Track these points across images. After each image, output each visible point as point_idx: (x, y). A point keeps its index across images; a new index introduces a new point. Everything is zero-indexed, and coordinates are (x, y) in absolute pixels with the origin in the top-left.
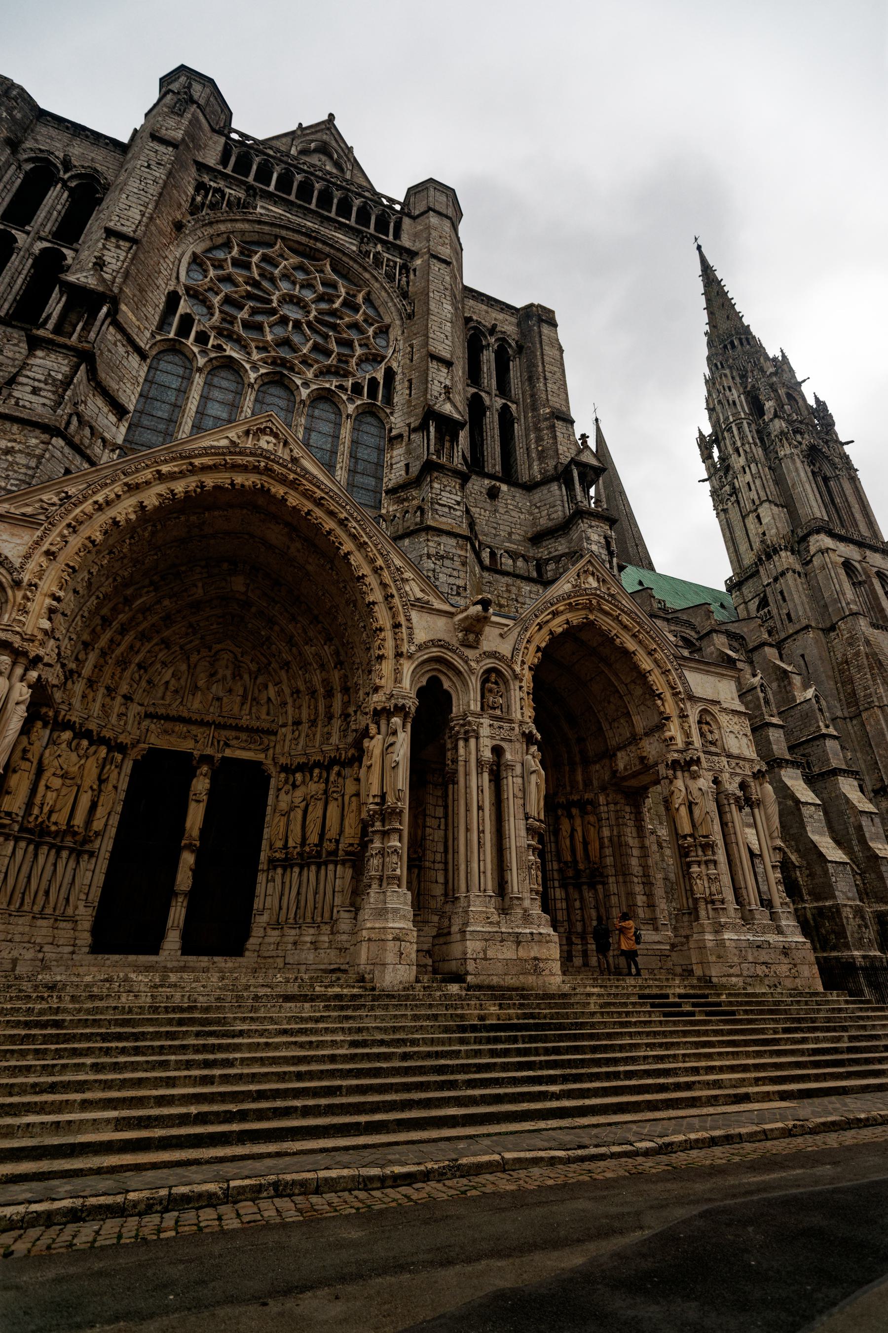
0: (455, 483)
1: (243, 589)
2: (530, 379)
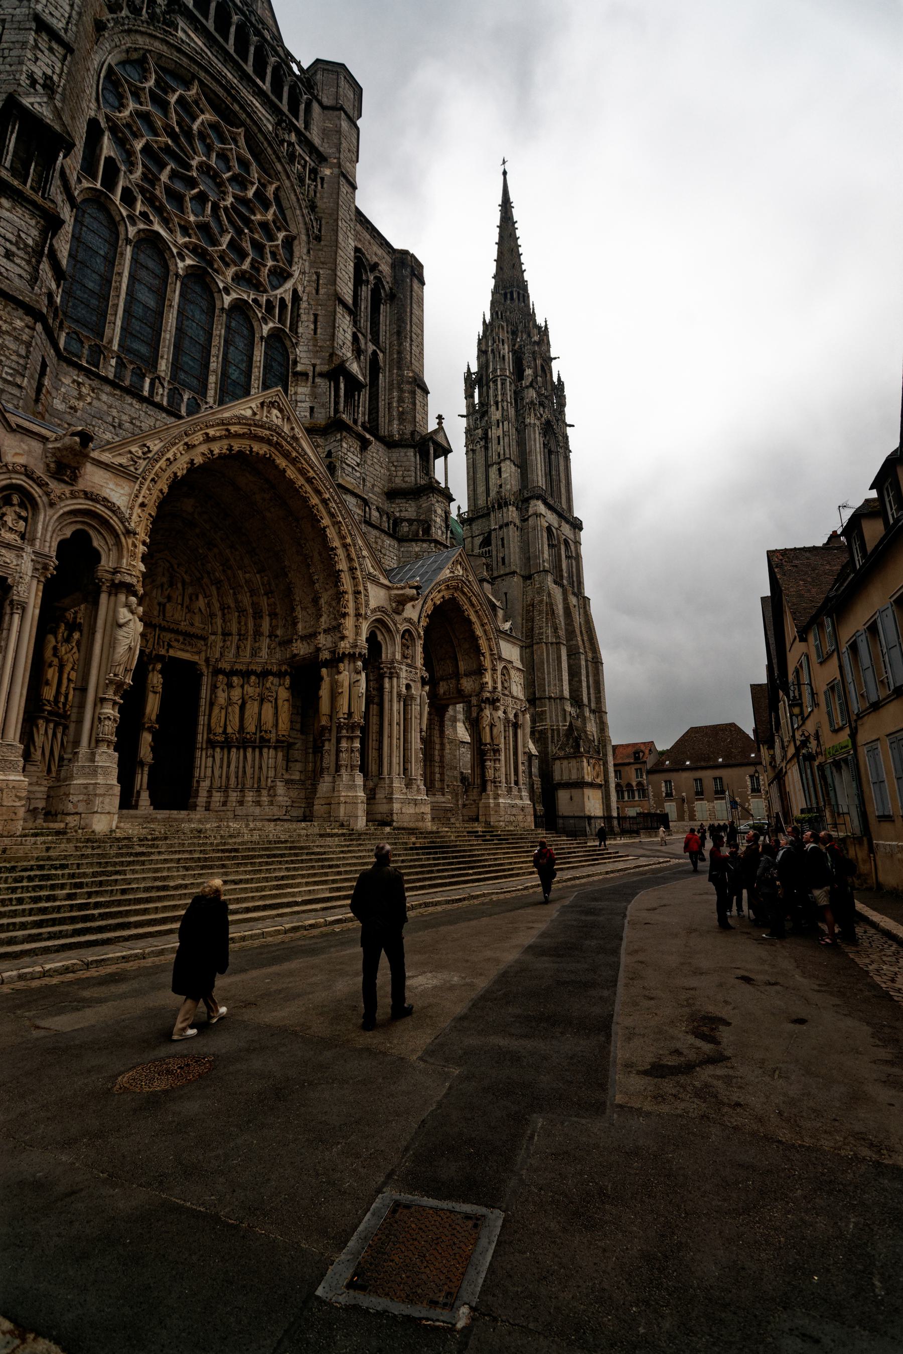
0: (356, 445)
2: (399, 333)
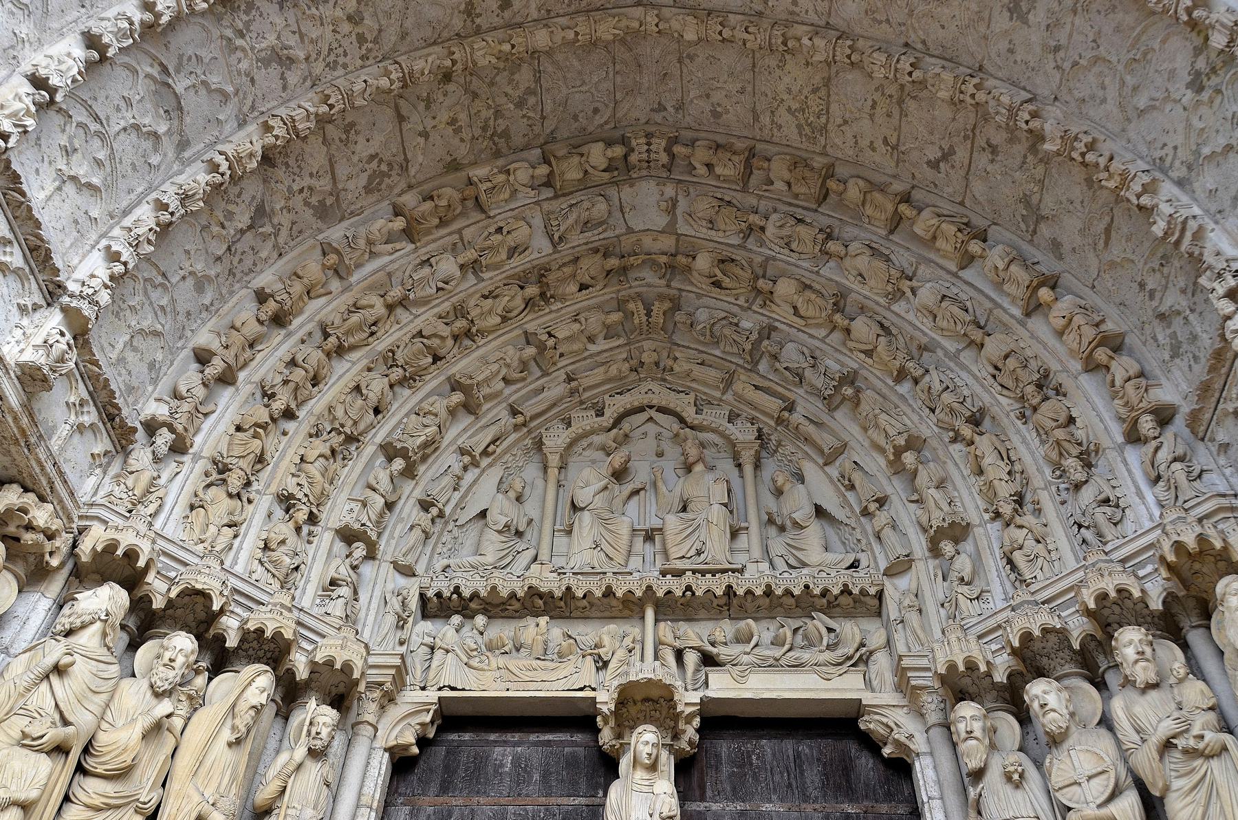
1: (661, 221)
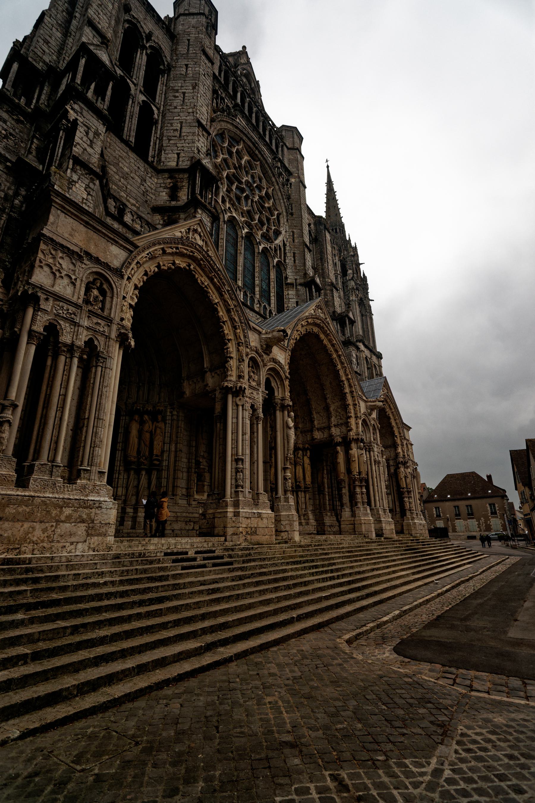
2: (321, 259)
